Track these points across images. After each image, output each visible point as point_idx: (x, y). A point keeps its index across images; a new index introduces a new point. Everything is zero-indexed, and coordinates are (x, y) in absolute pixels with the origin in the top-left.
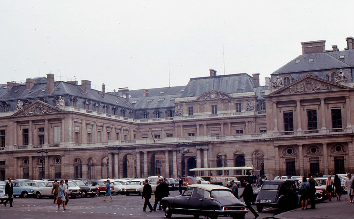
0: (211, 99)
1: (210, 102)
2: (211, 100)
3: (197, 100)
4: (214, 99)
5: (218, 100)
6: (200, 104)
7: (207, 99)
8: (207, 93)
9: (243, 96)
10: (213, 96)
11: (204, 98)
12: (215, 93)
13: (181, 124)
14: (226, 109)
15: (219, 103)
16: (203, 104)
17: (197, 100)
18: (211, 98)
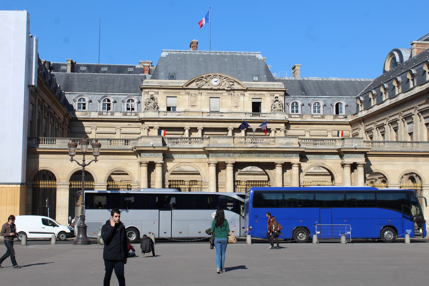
0: (212, 87)
2: (211, 89)
3: (186, 86)
4: (216, 88)
5: (224, 90)
7: (203, 87)
8: (204, 76)
9: (267, 87)
10: (214, 82)
12: (219, 77)
13: (157, 125)
14: (236, 105)
16: (195, 94)
17: (186, 86)
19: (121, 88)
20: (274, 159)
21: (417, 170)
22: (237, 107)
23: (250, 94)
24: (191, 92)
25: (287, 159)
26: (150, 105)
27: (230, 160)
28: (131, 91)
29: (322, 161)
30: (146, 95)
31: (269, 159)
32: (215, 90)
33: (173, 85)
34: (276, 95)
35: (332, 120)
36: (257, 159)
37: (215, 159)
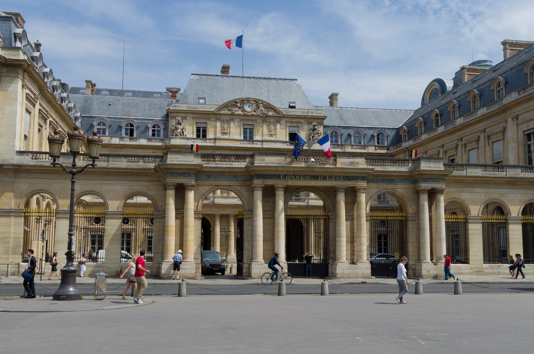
1: (243, 118)
3: (218, 111)
6: (222, 119)
7: (237, 113)
11: (229, 110)
15: (258, 121)
16: (227, 120)
17: (218, 111)
18: (244, 110)
19: (146, 112)
20: (335, 183)
21: (502, 199)
22: (271, 135)
23: (286, 122)
24: (223, 118)
25: (350, 183)
26: (179, 130)
27: (280, 183)
28: (157, 116)
29: (393, 186)
30: (173, 120)
31: (328, 183)
32: (249, 115)
33: (203, 110)
34: (314, 124)
35: (373, 152)
36: (314, 182)
37: (261, 181)
